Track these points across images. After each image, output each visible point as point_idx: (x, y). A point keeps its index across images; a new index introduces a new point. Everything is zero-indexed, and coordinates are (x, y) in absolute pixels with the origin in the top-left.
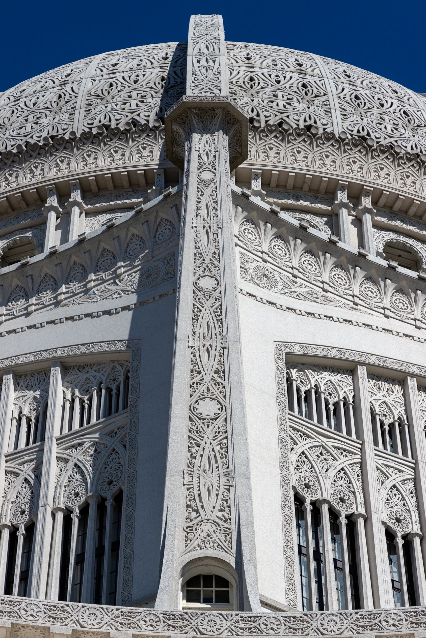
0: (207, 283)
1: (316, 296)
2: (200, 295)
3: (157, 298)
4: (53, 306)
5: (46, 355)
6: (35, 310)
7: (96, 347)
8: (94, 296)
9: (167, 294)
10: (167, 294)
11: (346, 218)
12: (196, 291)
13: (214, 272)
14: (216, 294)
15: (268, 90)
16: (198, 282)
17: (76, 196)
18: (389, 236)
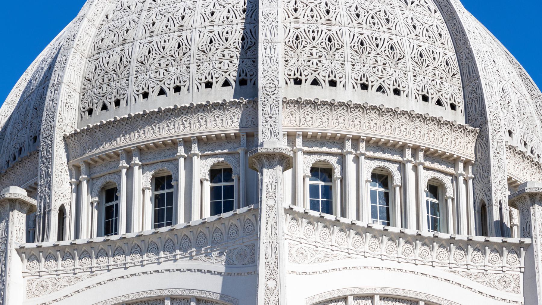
0: (271, 284)
1: (328, 256)
2: (268, 292)
3: (246, 274)
4: (189, 258)
5: (188, 293)
6: (180, 258)
7: (214, 295)
8: (212, 258)
9: (250, 273)
10: (250, 273)
11: (350, 158)
12: (266, 290)
13: (275, 276)
14: (276, 291)
15: (307, 49)
16: (267, 283)
17: (195, 148)
18: (375, 164)
